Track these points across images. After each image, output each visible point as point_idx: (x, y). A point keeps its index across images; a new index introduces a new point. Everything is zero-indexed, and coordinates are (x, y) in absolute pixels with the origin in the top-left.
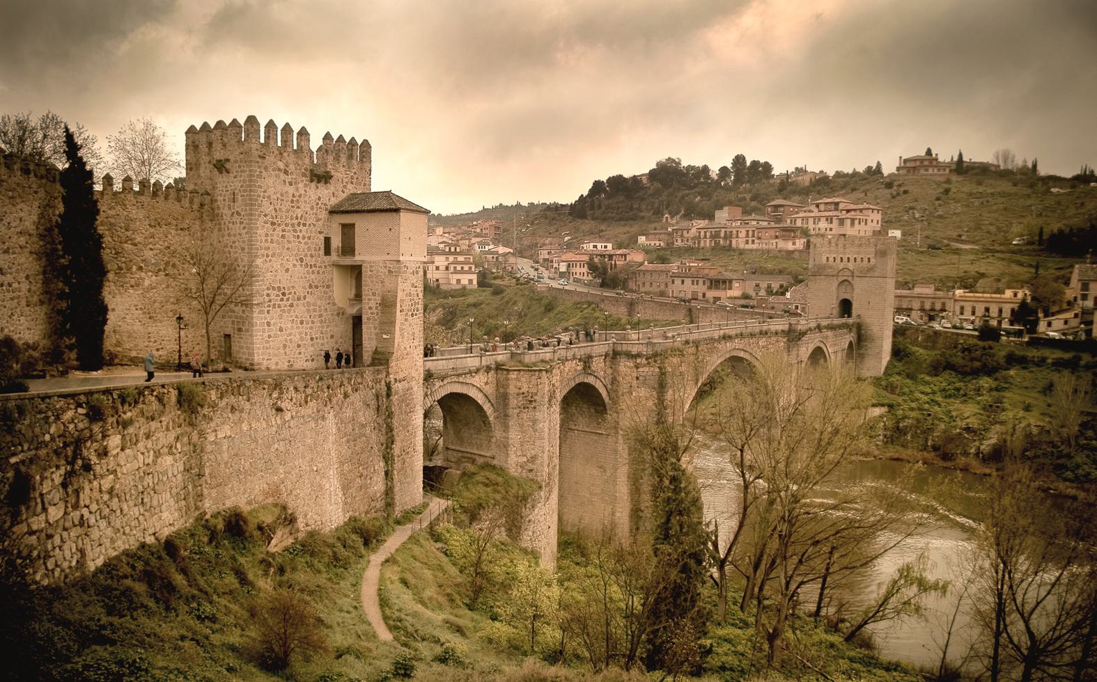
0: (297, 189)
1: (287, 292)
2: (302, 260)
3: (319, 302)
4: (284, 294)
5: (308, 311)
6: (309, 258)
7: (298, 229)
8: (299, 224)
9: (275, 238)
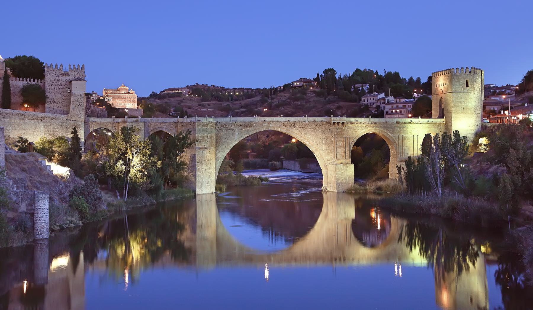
0: (59, 78)
1: (55, 101)
2: (60, 94)
3: (66, 104)
4: (55, 101)
5: (62, 105)
6: (63, 93)
7: (59, 87)
8: (60, 86)
9: (52, 89)
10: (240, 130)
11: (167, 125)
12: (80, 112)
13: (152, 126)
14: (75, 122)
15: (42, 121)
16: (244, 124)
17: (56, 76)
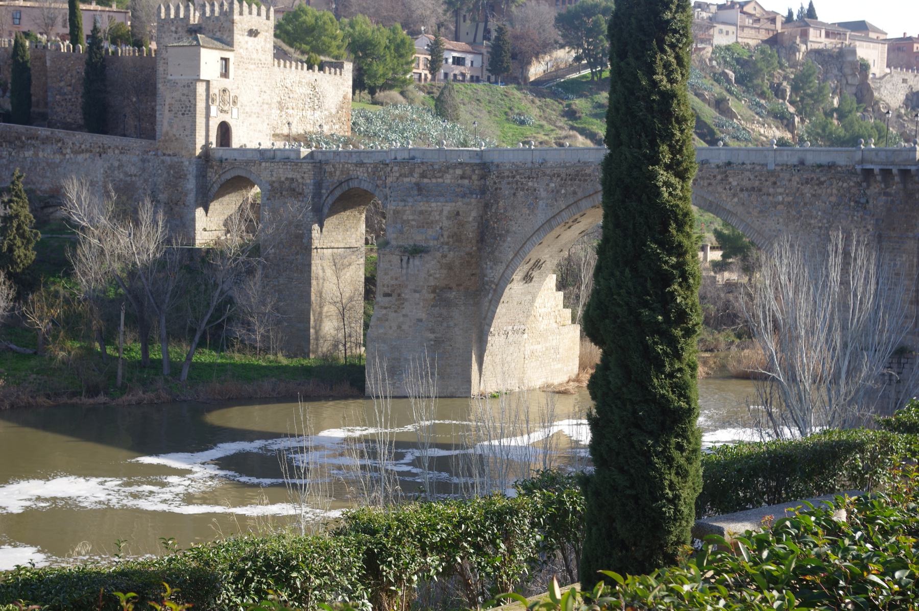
10: (553, 191)
11: (370, 170)
12: (186, 133)
13: (338, 173)
14: (175, 159)
15: (100, 156)
16: (563, 171)
17: (177, 36)
